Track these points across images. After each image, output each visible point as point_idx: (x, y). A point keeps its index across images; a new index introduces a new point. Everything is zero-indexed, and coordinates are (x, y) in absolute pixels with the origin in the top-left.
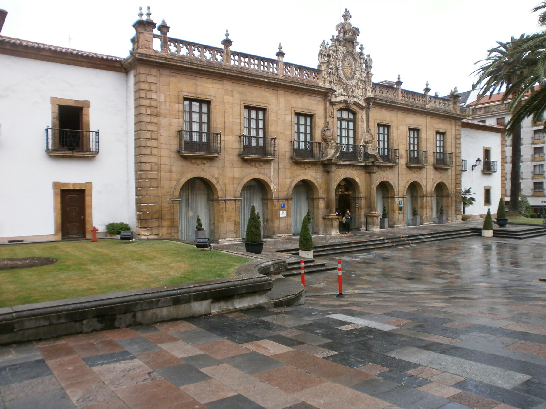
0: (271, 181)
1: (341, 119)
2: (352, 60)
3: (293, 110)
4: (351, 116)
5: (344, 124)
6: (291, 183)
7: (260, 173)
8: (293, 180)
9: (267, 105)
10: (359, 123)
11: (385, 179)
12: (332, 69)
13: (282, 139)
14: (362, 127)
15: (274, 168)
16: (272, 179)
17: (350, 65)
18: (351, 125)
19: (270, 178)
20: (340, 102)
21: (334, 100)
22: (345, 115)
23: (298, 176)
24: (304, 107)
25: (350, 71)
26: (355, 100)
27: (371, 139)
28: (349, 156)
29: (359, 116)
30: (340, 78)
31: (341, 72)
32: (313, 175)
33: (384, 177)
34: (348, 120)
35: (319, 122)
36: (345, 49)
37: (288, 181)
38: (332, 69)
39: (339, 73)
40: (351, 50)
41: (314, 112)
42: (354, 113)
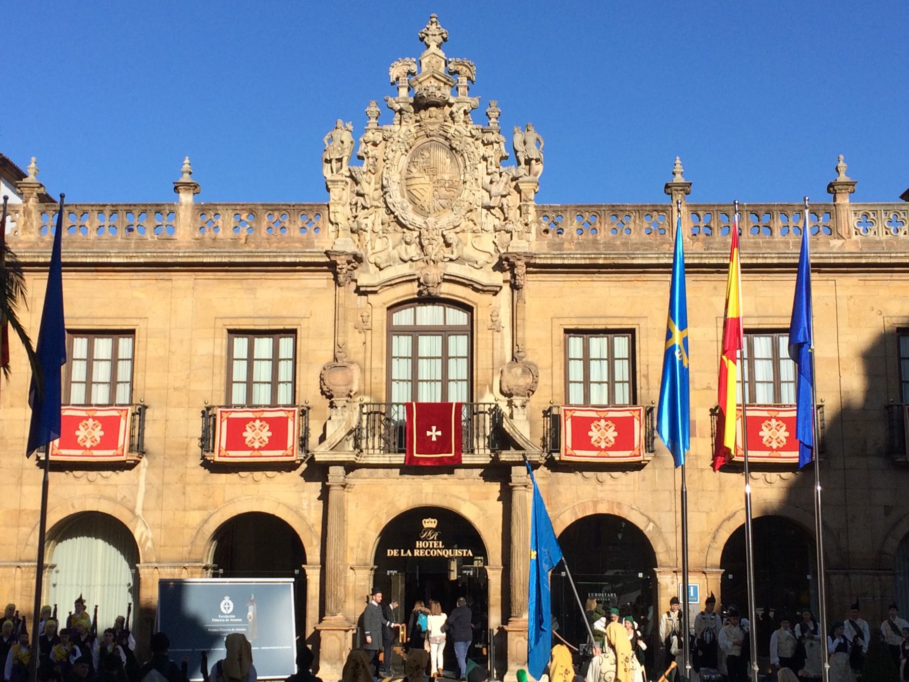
0: (136, 517)
1: (415, 332)
2: (442, 156)
3: (219, 323)
4: (458, 318)
5: (429, 345)
6: (206, 521)
7: (102, 497)
8: (211, 515)
9: (135, 322)
10: (482, 335)
11: (603, 509)
12: (362, 195)
13: (179, 405)
14: (494, 347)
15: (148, 483)
16: (139, 511)
17: (431, 170)
18: (458, 345)
19: (132, 511)
20: (390, 284)
21: (364, 279)
22: (429, 315)
23: (231, 501)
24: (262, 314)
25: (430, 189)
26: (455, 269)
27: (525, 381)
28: (428, 436)
29: (481, 315)
30: (393, 213)
31: (396, 197)
32: (287, 498)
33: (595, 503)
34: (444, 332)
35: (317, 350)
36: (413, 130)
37: (195, 518)
38: (362, 195)
39: (389, 200)
40: (437, 127)
41: (296, 321)
42: (467, 308)
